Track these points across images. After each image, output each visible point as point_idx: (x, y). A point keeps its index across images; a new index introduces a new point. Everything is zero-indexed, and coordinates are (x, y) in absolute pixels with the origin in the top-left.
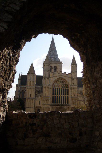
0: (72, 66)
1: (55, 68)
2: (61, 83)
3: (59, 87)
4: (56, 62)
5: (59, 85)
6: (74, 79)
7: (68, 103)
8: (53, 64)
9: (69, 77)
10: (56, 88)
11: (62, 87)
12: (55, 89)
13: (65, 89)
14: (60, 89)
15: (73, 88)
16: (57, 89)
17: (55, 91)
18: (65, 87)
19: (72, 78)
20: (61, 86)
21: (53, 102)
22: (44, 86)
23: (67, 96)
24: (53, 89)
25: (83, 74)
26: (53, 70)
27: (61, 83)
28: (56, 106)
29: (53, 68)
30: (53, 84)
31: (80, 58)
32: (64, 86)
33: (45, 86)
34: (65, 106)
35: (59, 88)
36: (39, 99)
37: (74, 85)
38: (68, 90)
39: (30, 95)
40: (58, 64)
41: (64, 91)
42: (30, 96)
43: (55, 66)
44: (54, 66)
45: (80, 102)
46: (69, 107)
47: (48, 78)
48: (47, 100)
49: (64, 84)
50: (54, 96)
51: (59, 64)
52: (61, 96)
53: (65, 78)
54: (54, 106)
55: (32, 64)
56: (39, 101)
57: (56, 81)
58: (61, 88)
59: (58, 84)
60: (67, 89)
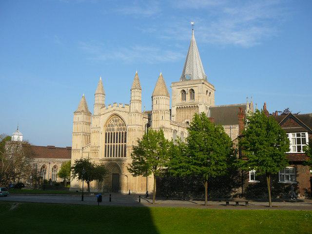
4: (191, 82)
7: (125, 156)
8: (187, 86)
11: (118, 129)
12: (109, 133)
14: (114, 133)
15: (131, 130)
17: (109, 137)
18: (121, 129)
20: (116, 128)
21: (105, 156)
23: (124, 144)
24: (106, 133)
26: (188, 97)
38: (126, 133)
43: (190, 88)
48: (96, 152)
49: (120, 125)
50: (107, 144)
52: (113, 144)
53: (120, 114)
57: (109, 119)
60: (124, 132)
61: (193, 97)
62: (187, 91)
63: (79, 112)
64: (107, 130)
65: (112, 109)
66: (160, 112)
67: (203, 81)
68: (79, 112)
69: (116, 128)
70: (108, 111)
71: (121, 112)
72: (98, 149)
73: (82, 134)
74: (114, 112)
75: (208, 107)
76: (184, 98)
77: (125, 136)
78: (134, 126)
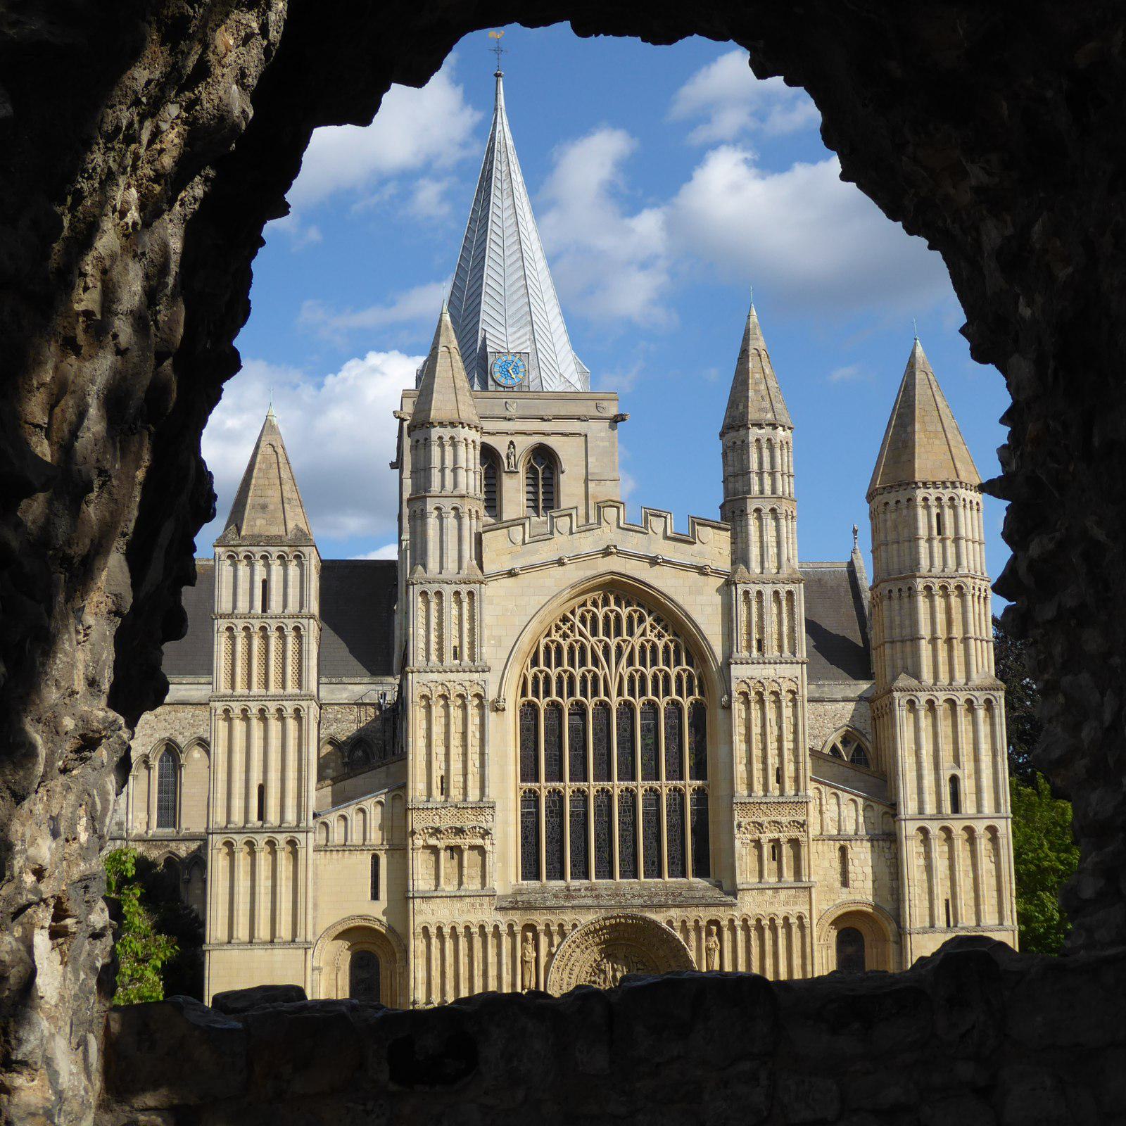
0: (731, 435)
2: (613, 643)
5: (596, 662)
6: (768, 591)
9: (702, 571)
10: (566, 703)
11: (637, 685)
13: (662, 702)
15: (757, 697)
16: (580, 710)
20: (615, 673)
21: (530, 869)
22: (418, 684)
24: (529, 713)
25: (1007, 503)
26: (515, 492)
27: (613, 643)
29: (522, 469)
31: (963, 320)
32: (649, 672)
33: (435, 676)
34: (674, 913)
35: (590, 703)
37: (772, 652)
39: (262, 790)
41: (651, 731)
43: (536, 440)
44: (524, 444)
45: (843, 850)
46: (723, 915)
47: (464, 589)
49: (648, 654)
50: (544, 787)
53: (663, 581)
54: (540, 919)
58: (615, 702)
59: (580, 655)
64: (540, 685)
69: (615, 673)
70: (546, 552)
71: (666, 569)
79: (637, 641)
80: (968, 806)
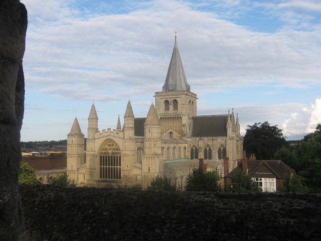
1: (175, 101)
3: (108, 153)
11: (113, 153)
12: (104, 157)
13: (116, 156)
15: (126, 155)
19: (123, 139)
21: (101, 177)
24: (101, 157)
26: (171, 107)
28: (103, 183)
30: (100, 149)
34: (115, 184)
35: (107, 156)
36: (83, 172)
38: (120, 157)
40: (180, 95)
42: (71, 168)
49: (114, 149)
50: (102, 166)
51: (180, 96)
52: (108, 167)
53: (115, 139)
55: (76, 120)
56: (83, 175)
57: (103, 144)
59: (106, 149)
61: (176, 107)
62: (171, 100)
63: (73, 135)
64: (102, 153)
65: (106, 134)
66: (152, 140)
67: (186, 93)
68: (73, 135)
69: (110, 152)
70: (101, 136)
72: (94, 171)
73: (76, 156)
74: (109, 137)
75: (191, 117)
76: (167, 108)
77: (120, 160)
78: (129, 152)
79: (112, 148)
80: (150, 171)
